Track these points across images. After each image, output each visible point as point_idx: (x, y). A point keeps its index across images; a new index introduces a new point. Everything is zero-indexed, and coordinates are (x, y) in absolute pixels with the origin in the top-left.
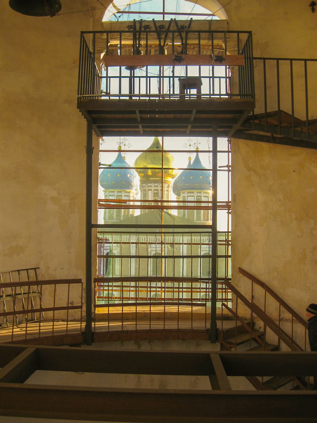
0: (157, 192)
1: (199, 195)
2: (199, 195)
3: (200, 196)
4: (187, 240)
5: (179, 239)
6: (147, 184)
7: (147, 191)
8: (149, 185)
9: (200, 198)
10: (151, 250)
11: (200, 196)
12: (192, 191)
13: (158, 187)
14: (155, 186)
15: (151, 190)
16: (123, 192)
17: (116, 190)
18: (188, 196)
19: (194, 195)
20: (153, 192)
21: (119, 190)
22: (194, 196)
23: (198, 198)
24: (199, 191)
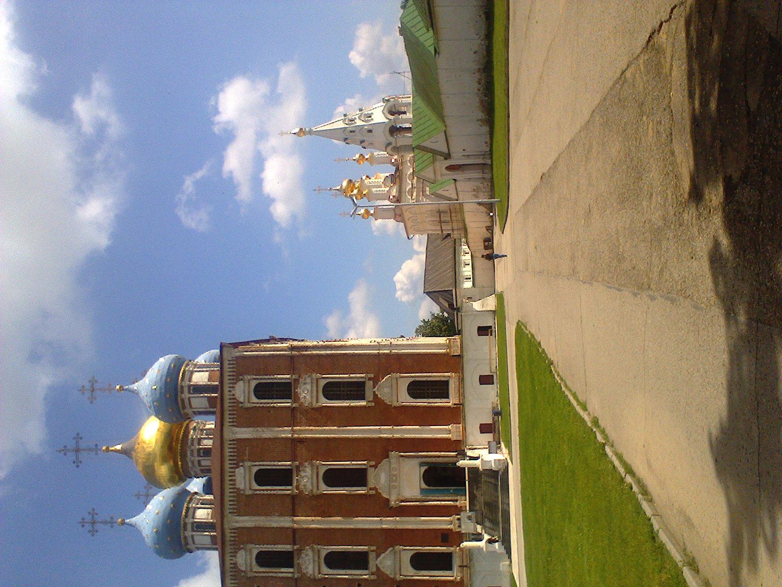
0: (202, 451)
1: (186, 390)
2: (186, 390)
4: (231, 427)
5: (230, 441)
7: (202, 468)
8: (190, 465)
9: (192, 388)
10: (250, 489)
11: (189, 386)
12: (180, 401)
13: (192, 451)
14: (192, 455)
16: (187, 520)
17: (182, 534)
18: (191, 407)
19: (187, 400)
20: (202, 458)
21: (182, 528)
22: (189, 399)
23: (192, 392)
24: (179, 390)
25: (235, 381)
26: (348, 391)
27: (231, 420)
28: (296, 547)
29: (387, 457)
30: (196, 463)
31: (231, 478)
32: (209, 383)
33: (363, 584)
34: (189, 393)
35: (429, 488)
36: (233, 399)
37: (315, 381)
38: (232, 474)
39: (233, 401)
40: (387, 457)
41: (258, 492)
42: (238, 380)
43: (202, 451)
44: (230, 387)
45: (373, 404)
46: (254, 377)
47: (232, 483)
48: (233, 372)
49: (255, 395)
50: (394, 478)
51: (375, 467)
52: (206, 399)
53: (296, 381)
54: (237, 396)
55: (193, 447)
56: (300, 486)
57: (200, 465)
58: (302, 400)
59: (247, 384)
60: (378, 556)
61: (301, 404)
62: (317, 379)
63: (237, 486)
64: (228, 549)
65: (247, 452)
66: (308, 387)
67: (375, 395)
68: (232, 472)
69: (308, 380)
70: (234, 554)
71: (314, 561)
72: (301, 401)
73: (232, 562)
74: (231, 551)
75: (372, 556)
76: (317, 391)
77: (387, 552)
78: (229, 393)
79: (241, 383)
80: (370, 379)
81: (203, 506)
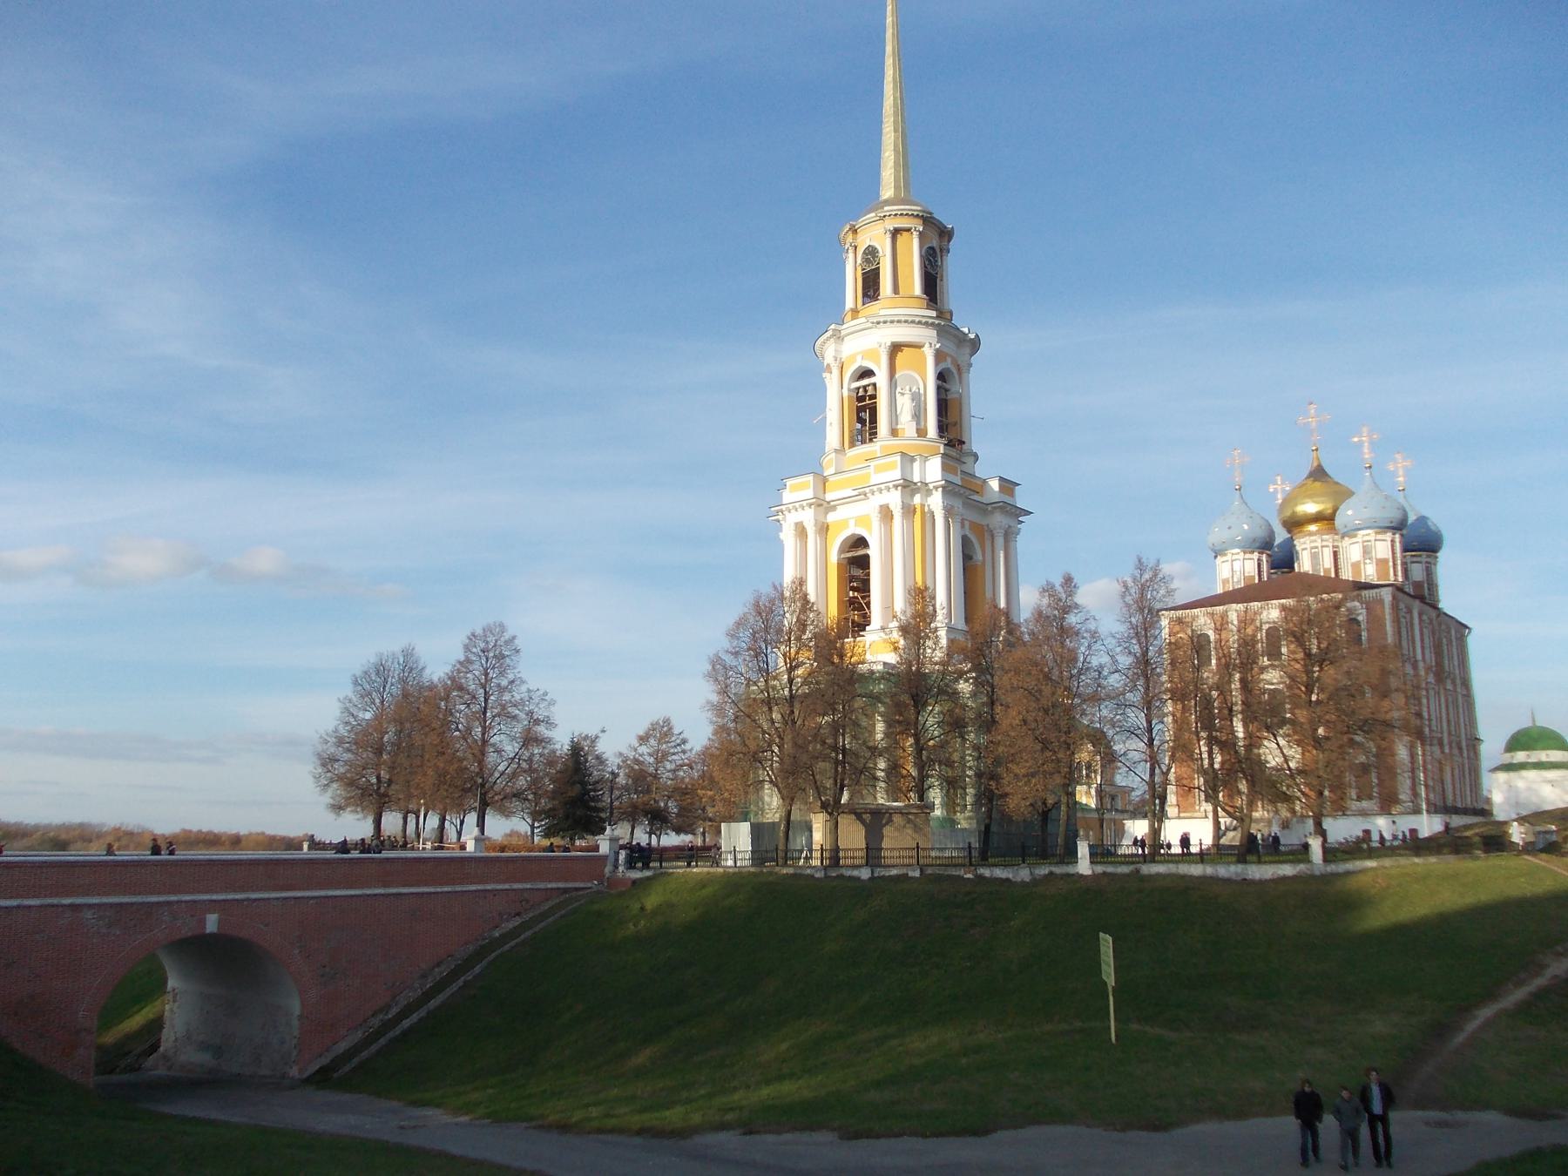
8: (1302, 540)
13: (1315, 541)
14: (1312, 542)
15: (1305, 549)
30: (1304, 546)
43: (1316, 550)
55: (1320, 541)
57: (1303, 549)
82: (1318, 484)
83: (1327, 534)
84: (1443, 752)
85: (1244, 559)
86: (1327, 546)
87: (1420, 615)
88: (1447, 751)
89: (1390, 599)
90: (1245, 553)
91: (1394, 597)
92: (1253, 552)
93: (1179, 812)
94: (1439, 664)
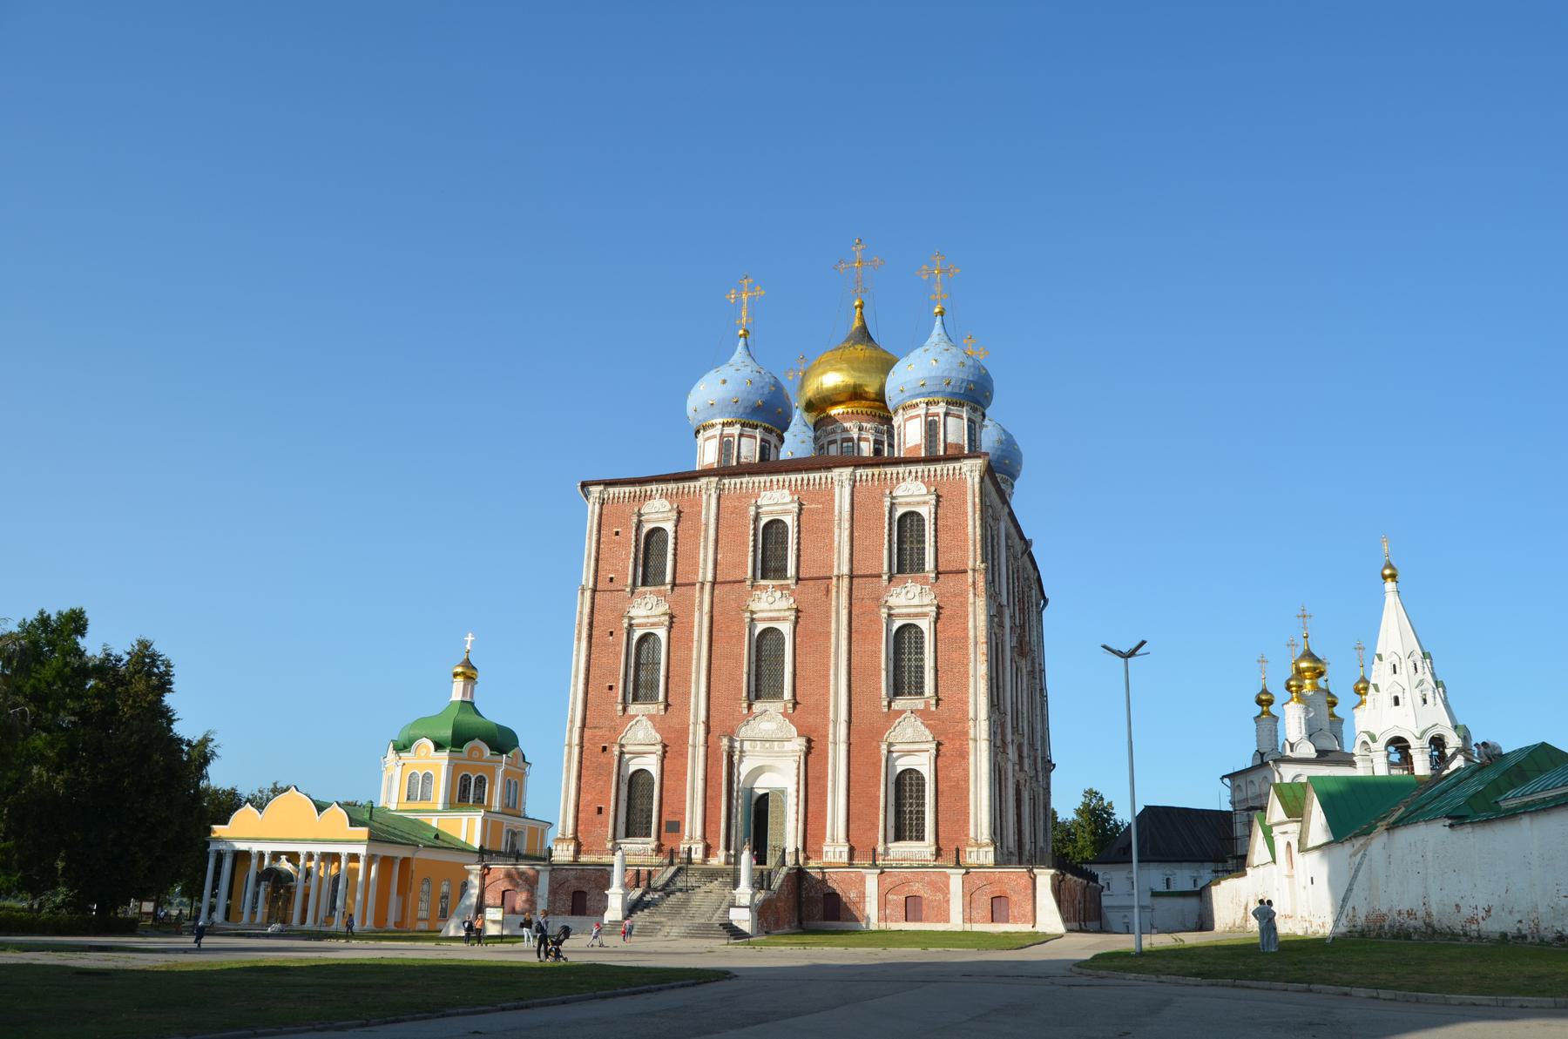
3: (938, 415)
5: (832, 479)
6: (824, 428)
7: (826, 446)
8: (830, 428)
9: (936, 418)
15: (835, 442)
18: (906, 421)
20: (839, 446)
22: (918, 416)
23: (930, 418)
25: (926, 480)
26: (910, 667)
27: (864, 477)
28: (669, 587)
29: (799, 735)
30: (831, 438)
31: (775, 483)
32: (942, 445)
33: (612, 693)
34: (927, 415)
35: (753, 802)
36: (897, 478)
37: (925, 610)
38: (781, 483)
39: (894, 479)
40: (799, 735)
41: (752, 527)
42: (928, 485)
43: (850, 444)
44: (917, 472)
45: (886, 710)
46: (933, 510)
47: (768, 484)
48: (942, 475)
49: (904, 516)
50: (767, 745)
51: (785, 714)
52: (919, 442)
53: (925, 581)
54: (903, 485)
56: (758, 592)
58: (895, 590)
59: (922, 499)
60: (651, 717)
61: (887, 589)
62: (925, 615)
63: (763, 494)
64: (672, 486)
65: (813, 506)
66: (916, 601)
67: (900, 713)
68: (783, 485)
69: (926, 600)
70: (666, 495)
71: (648, 617)
72: (892, 589)
73: (654, 492)
74: (670, 490)
75: (652, 709)
76: (908, 615)
77: (653, 732)
78: (907, 471)
79: (924, 491)
80: (927, 704)
81: (758, 449)
82: (859, 347)
83: (868, 422)
84: (1021, 769)
85: (741, 435)
86: (867, 440)
87: (1007, 537)
88: (1026, 767)
89: (977, 479)
90: (743, 425)
91: (982, 479)
92: (756, 427)
93: (578, 852)
94: (1022, 627)
